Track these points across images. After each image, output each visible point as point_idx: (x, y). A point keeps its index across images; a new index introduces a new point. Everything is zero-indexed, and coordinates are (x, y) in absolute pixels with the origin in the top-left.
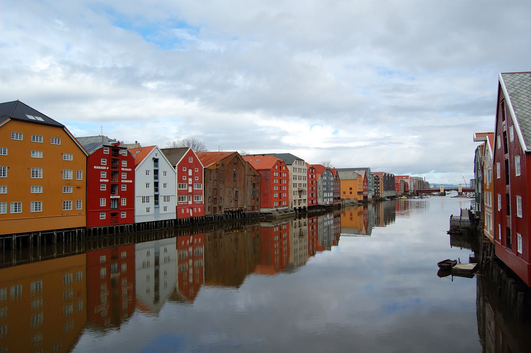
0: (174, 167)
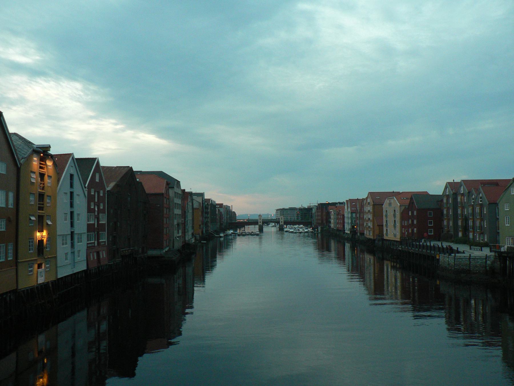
0: (85, 187)
